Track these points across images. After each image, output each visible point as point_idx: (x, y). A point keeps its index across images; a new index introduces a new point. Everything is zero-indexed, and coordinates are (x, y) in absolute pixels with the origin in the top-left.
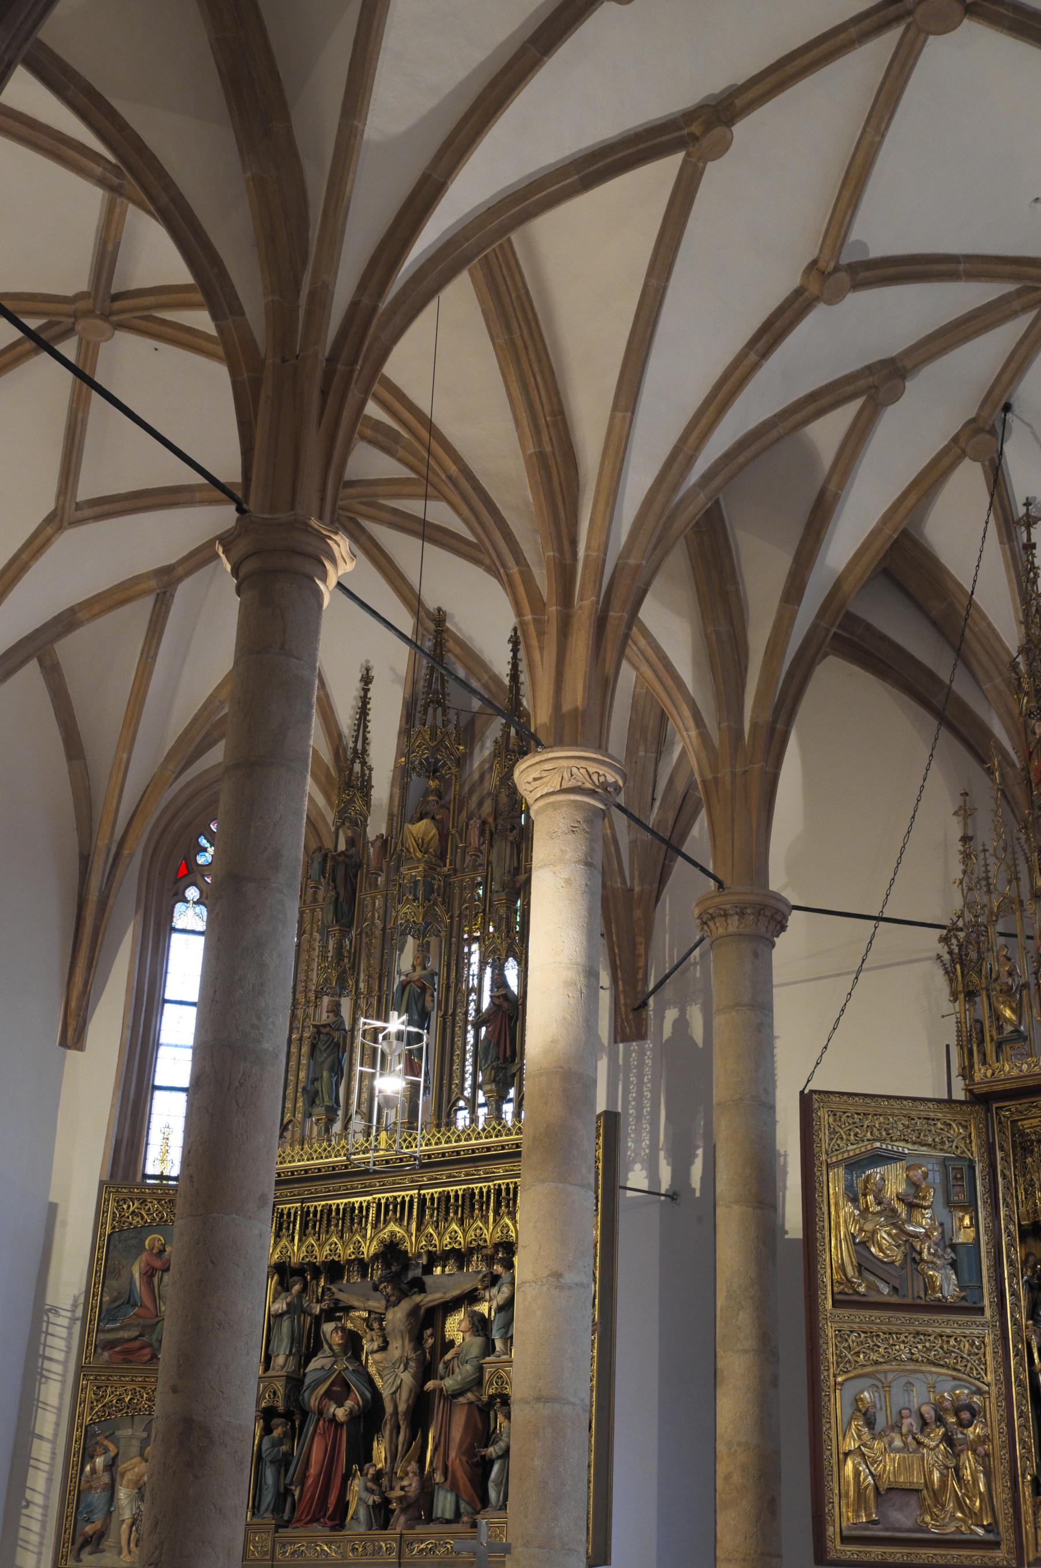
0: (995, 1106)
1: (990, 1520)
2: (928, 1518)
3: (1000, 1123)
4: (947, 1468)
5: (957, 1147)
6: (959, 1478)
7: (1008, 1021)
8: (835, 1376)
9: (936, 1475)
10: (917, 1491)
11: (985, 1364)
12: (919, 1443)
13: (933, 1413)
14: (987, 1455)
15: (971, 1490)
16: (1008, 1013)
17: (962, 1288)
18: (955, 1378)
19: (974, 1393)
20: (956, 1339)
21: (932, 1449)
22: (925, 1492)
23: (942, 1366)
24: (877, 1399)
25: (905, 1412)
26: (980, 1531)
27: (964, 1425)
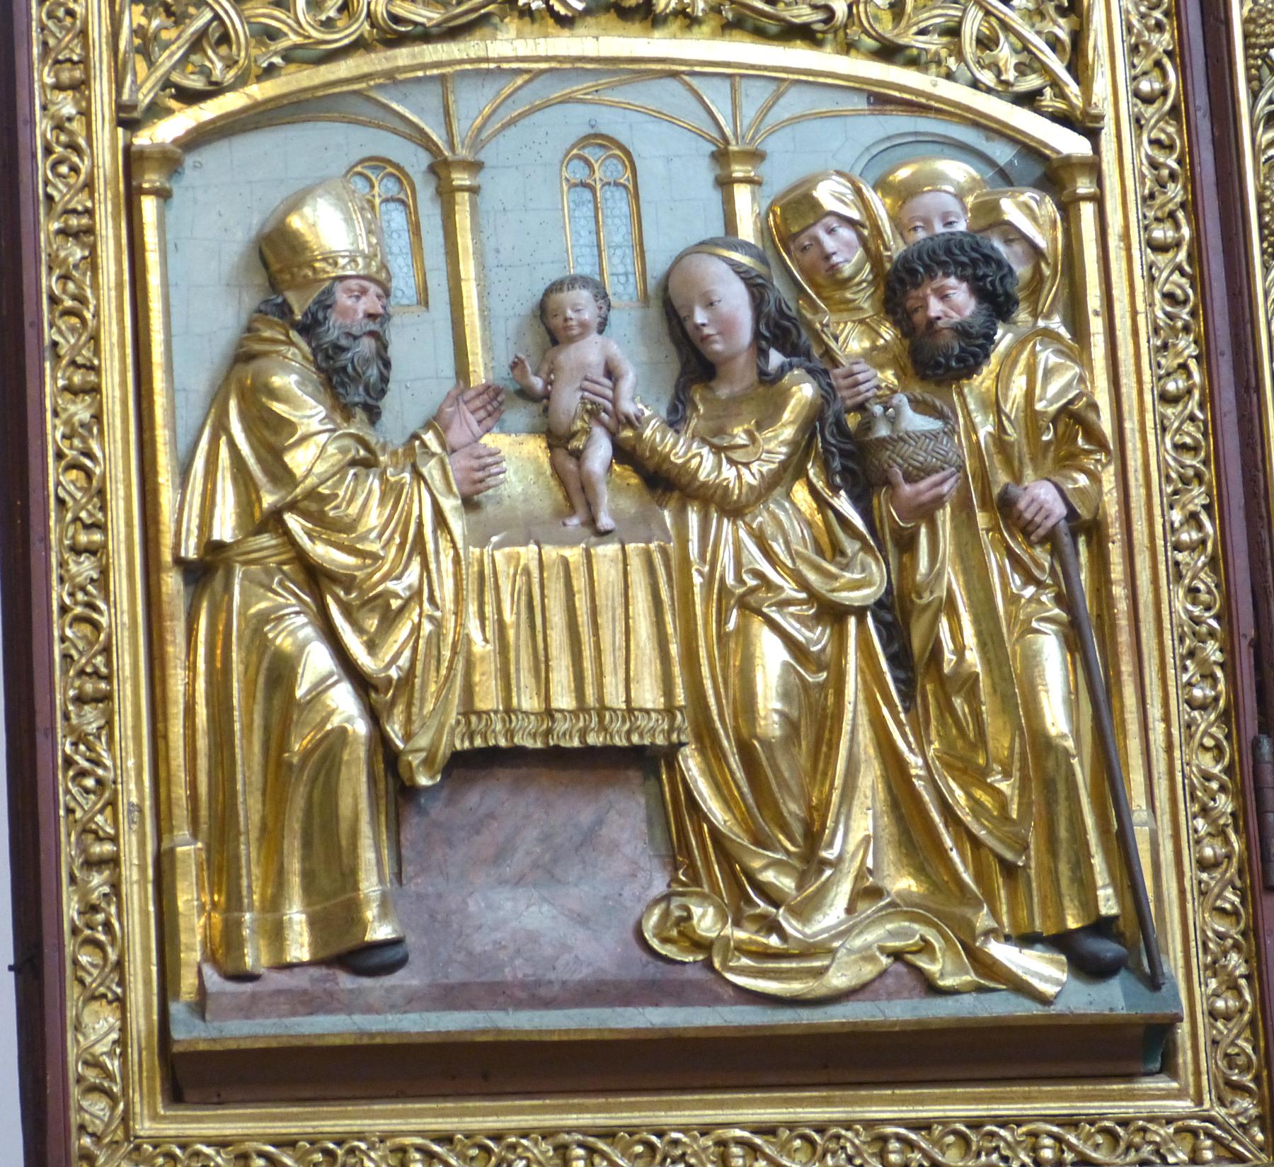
2: (706, 921)
4: (832, 614)
8: (128, 119)
9: (770, 657)
10: (646, 762)
12: (662, 482)
13: (735, 300)
14: (1088, 527)
18: (881, 100)
19: (1005, 177)
21: (735, 511)
22: (692, 764)
24: (400, 243)
25: (581, 305)
26: (1041, 969)
27: (938, 363)
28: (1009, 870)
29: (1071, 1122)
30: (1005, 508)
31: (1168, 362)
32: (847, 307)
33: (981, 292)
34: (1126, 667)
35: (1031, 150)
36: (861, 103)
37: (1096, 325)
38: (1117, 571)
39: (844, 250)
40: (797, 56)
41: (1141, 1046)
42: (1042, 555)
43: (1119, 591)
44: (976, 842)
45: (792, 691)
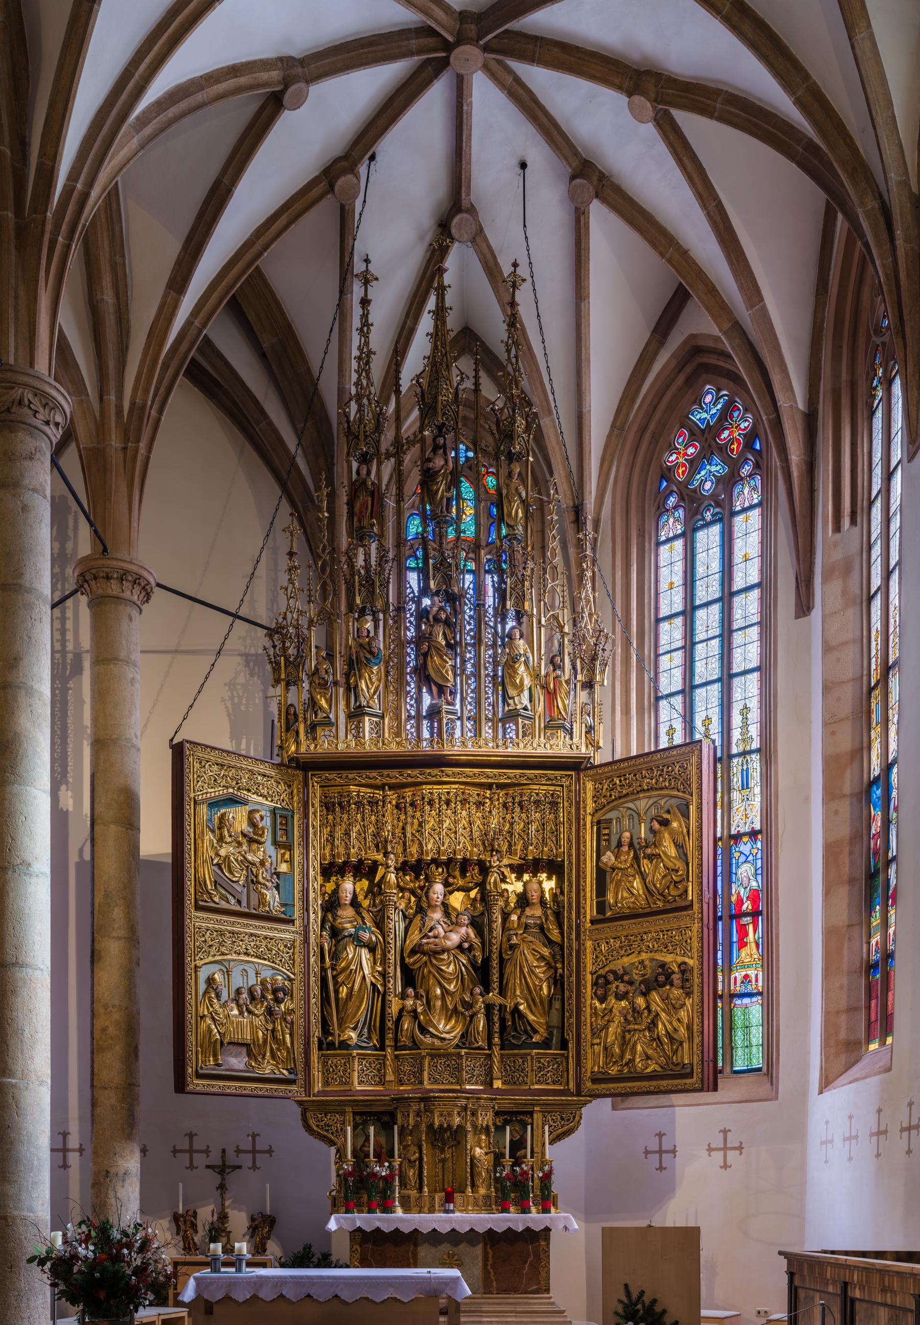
4: (267, 1030)
6: (274, 1037)
7: (321, 708)
12: (250, 1012)
13: (259, 992)
15: (281, 1043)
16: (323, 703)
18: (273, 968)
23: (265, 959)
27: (278, 1001)
30: (285, 1019)
35: (288, 976)
39: (269, 986)
40: (266, 962)
41: (293, 1082)
45: (263, 1038)
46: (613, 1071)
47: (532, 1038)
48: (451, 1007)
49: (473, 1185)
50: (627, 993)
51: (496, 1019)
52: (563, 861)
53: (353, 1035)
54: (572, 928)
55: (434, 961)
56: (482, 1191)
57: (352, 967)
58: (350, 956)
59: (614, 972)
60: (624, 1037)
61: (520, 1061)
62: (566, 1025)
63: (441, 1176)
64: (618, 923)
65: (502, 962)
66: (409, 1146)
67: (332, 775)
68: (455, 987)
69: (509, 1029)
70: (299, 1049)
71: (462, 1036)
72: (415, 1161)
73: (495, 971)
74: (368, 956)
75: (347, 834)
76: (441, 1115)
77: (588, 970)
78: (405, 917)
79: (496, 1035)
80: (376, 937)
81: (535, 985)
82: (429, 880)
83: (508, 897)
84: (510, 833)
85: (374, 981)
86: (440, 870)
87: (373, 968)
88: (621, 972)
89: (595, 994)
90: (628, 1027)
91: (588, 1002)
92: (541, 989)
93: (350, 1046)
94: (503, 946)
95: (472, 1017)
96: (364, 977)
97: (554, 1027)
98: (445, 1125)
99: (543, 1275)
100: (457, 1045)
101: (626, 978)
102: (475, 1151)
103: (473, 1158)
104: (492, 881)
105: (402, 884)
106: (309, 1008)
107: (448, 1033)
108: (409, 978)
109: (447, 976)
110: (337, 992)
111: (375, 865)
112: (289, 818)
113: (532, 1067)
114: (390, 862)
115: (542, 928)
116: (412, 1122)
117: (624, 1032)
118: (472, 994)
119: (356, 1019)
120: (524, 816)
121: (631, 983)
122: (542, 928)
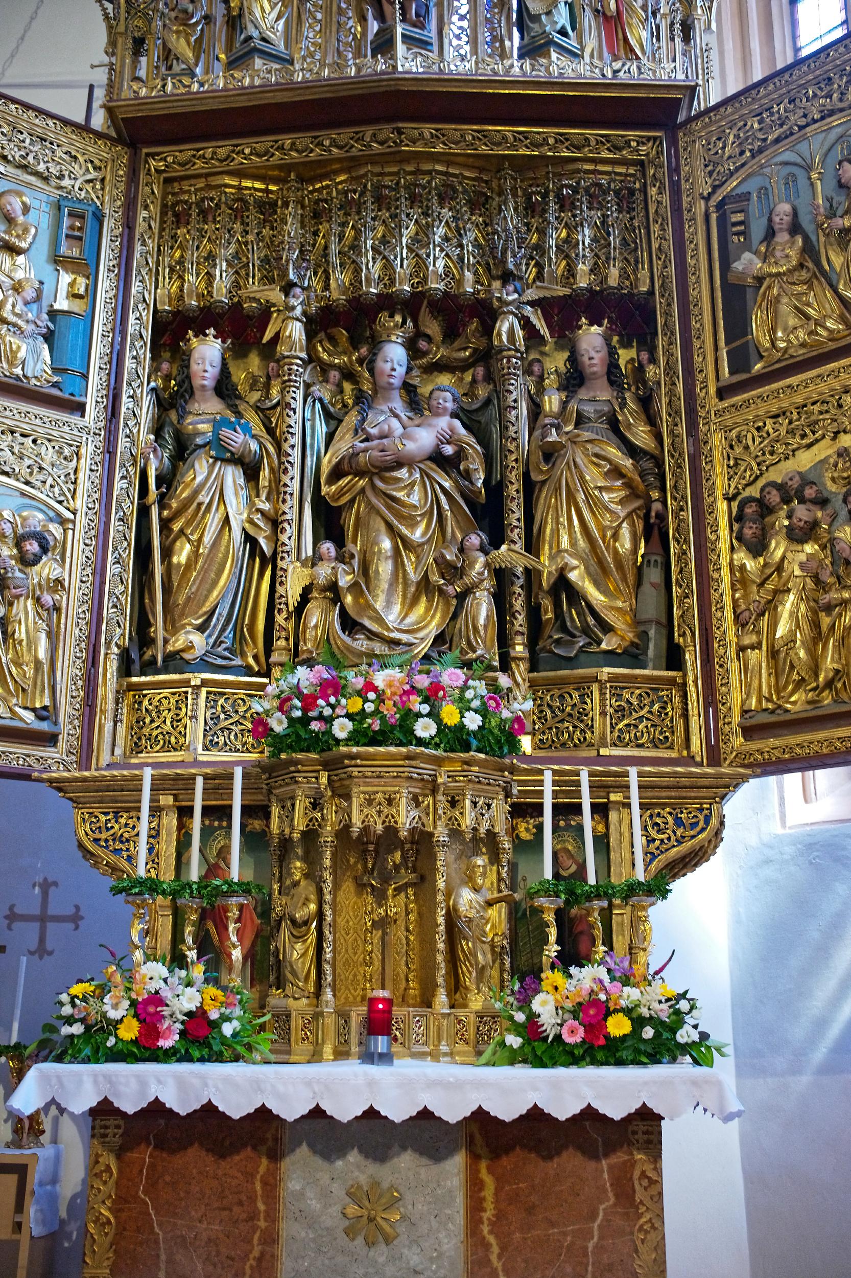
0: (145, 151)
1: (47, 702)
3: (149, 173)
5: (80, 189)
11: (75, 483)
17: (56, 370)
18: (23, 494)
19: (51, 520)
20: (34, 441)
26: (29, 716)
28: (24, 690)
29: (28, 756)
30: (38, 600)
31: (85, 573)
32: (6, 543)
33: (41, 546)
34: (61, 645)
35: (59, 515)
36: (18, 494)
37: (68, 561)
38: (63, 621)
39: (8, 531)
42: (45, 613)
43: (62, 626)
44: (16, 682)
46: (797, 702)
47: (599, 643)
48: (413, 575)
49: (456, 987)
50: (815, 524)
51: (518, 604)
52: (651, 292)
53: (197, 639)
54: (678, 413)
55: (379, 484)
56: (476, 1003)
57: (200, 498)
58: (199, 479)
59: (780, 487)
60: (815, 624)
61: (575, 695)
62: (676, 613)
63: (377, 963)
64: (781, 384)
65: (530, 489)
66: (296, 884)
67: (185, 152)
68: (424, 534)
69: (547, 632)
70: (69, 668)
71: (440, 639)
72: (306, 923)
73: (513, 506)
74: (241, 481)
75: (211, 258)
76: (370, 802)
77: (719, 492)
78: (328, 416)
79: (519, 639)
80: (261, 444)
81: (603, 530)
82: (376, 343)
83: (541, 378)
84: (540, 248)
85: (251, 531)
86: (398, 318)
87: (251, 504)
88: (795, 483)
89: (739, 539)
90: (826, 598)
91: (724, 563)
92: (615, 536)
93: (187, 662)
94: (533, 459)
95: (462, 597)
96: (227, 521)
97: (649, 621)
98: (380, 827)
99: (647, 1254)
100: (427, 658)
101: (809, 492)
102: (459, 896)
103: (452, 917)
104: (505, 327)
105: (325, 356)
106: (103, 583)
107: (407, 632)
108: (330, 523)
109: (405, 511)
110: (167, 553)
111: (265, 314)
112: (89, 216)
113: (603, 705)
114: (293, 302)
115: (614, 425)
116: (300, 823)
117: (815, 613)
118: (462, 550)
119: (205, 609)
120: (566, 216)
121: (822, 502)
122: (614, 425)
